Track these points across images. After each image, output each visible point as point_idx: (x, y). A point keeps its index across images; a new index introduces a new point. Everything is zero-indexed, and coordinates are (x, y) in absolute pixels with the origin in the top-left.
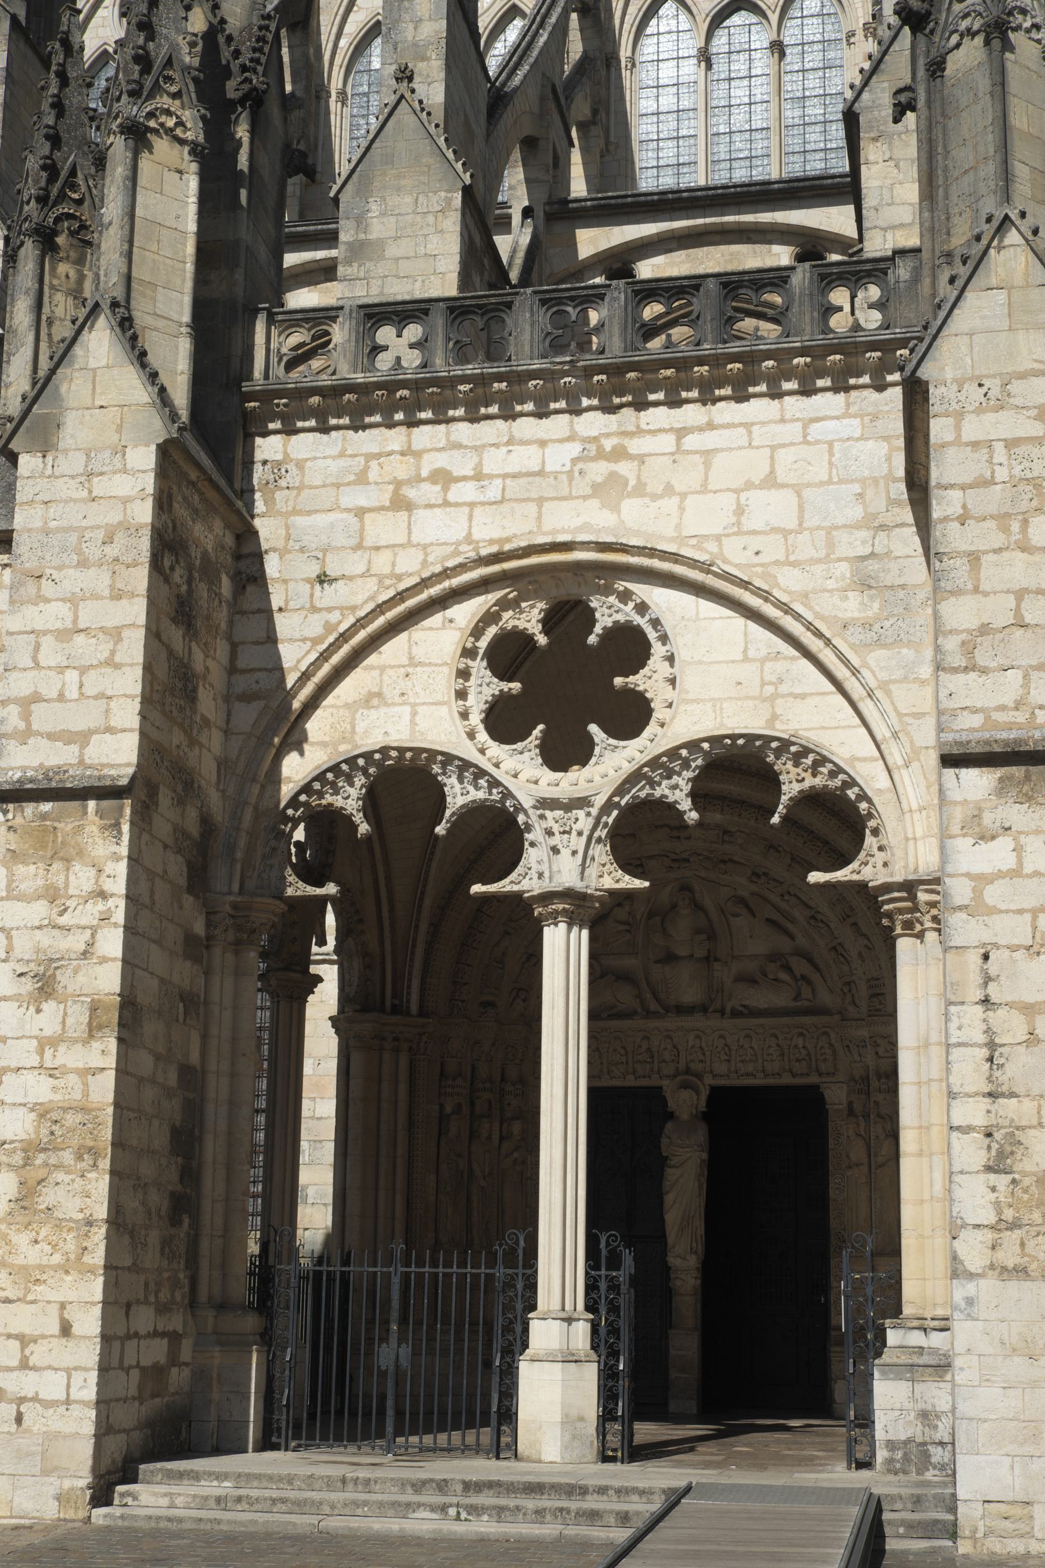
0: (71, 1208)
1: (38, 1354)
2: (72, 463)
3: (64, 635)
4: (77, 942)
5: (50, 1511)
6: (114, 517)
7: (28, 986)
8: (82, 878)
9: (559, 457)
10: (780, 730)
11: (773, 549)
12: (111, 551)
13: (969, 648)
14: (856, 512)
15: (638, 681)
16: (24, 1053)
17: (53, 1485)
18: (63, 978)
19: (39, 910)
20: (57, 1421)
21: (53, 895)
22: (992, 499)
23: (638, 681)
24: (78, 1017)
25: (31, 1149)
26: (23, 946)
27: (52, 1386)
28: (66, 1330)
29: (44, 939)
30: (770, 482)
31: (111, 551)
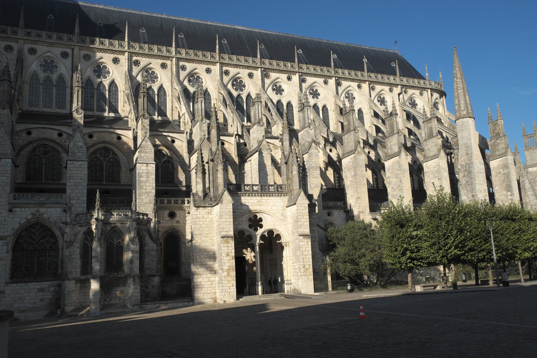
0: (232, 275)
1: (230, 288)
2: (225, 205)
3: (225, 222)
4: (230, 251)
5: (233, 301)
6: (229, 211)
7: (226, 255)
8: (230, 245)
9: (256, 201)
10: (275, 228)
11: (275, 212)
12: (229, 214)
13: (300, 226)
14: (281, 209)
15: (262, 223)
16: (226, 261)
17: (233, 299)
18: (229, 255)
19: (226, 248)
20: (233, 293)
21: (228, 247)
22: (301, 214)
23: (262, 223)
24: (231, 258)
25: (228, 270)
26: (225, 251)
27: (232, 290)
28: (233, 285)
29: (227, 251)
30: (274, 205)
31: (229, 214)
